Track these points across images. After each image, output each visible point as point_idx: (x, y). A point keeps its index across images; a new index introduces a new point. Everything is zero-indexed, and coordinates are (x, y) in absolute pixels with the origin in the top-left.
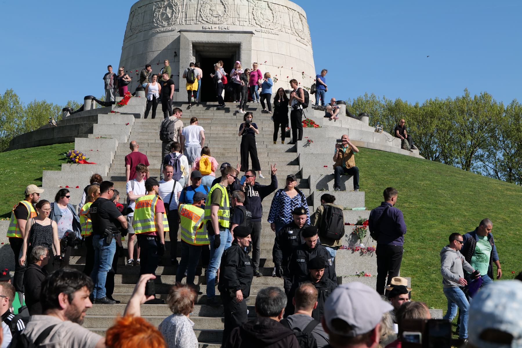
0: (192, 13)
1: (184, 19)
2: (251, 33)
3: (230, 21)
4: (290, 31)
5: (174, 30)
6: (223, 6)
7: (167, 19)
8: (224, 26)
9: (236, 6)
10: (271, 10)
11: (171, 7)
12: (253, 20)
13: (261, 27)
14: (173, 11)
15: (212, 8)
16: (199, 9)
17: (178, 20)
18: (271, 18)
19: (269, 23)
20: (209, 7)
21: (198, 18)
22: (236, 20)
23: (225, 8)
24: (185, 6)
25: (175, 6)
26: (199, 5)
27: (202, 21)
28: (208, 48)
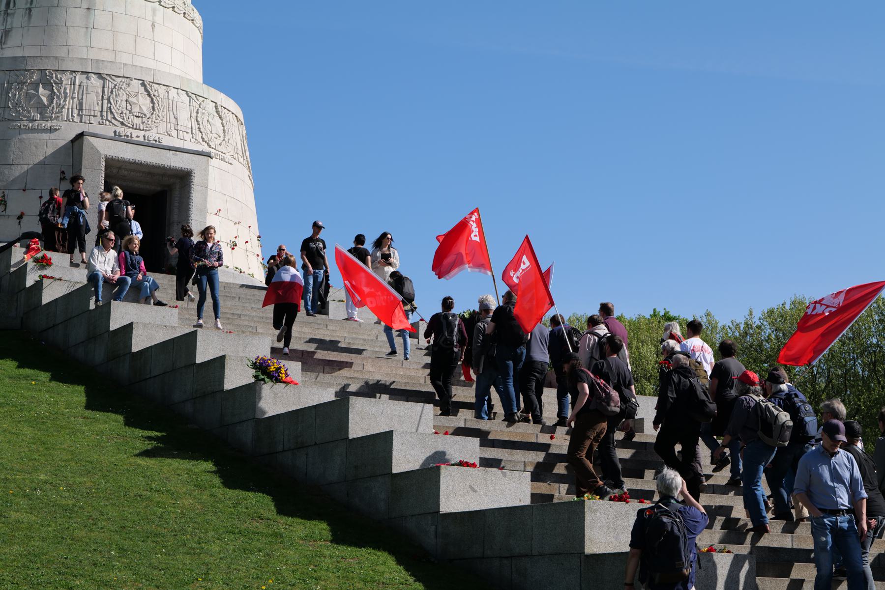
0: (92, 101)
1: (76, 111)
2: (209, 155)
3: (162, 127)
4: (241, 160)
5: (56, 130)
6: (149, 99)
7: (42, 109)
8: (153, 135)
9: (171, 102)
10: (220, 118)
11: (48, 85)
12: (198, 132)
13: (210, 146)
14: (52, 91)
15: (130, 99)
16: (106, 97)
17: (65, 111)
18: (221, 133)
19: (219, 142)
20: (125, 97)
21: (104, 114)
22: (173, 128)
23: (152, 102)
24: (77, 87)
25: (56, 83)
26: (106, 90)
27: (113, 121)
28: (126, 173)
